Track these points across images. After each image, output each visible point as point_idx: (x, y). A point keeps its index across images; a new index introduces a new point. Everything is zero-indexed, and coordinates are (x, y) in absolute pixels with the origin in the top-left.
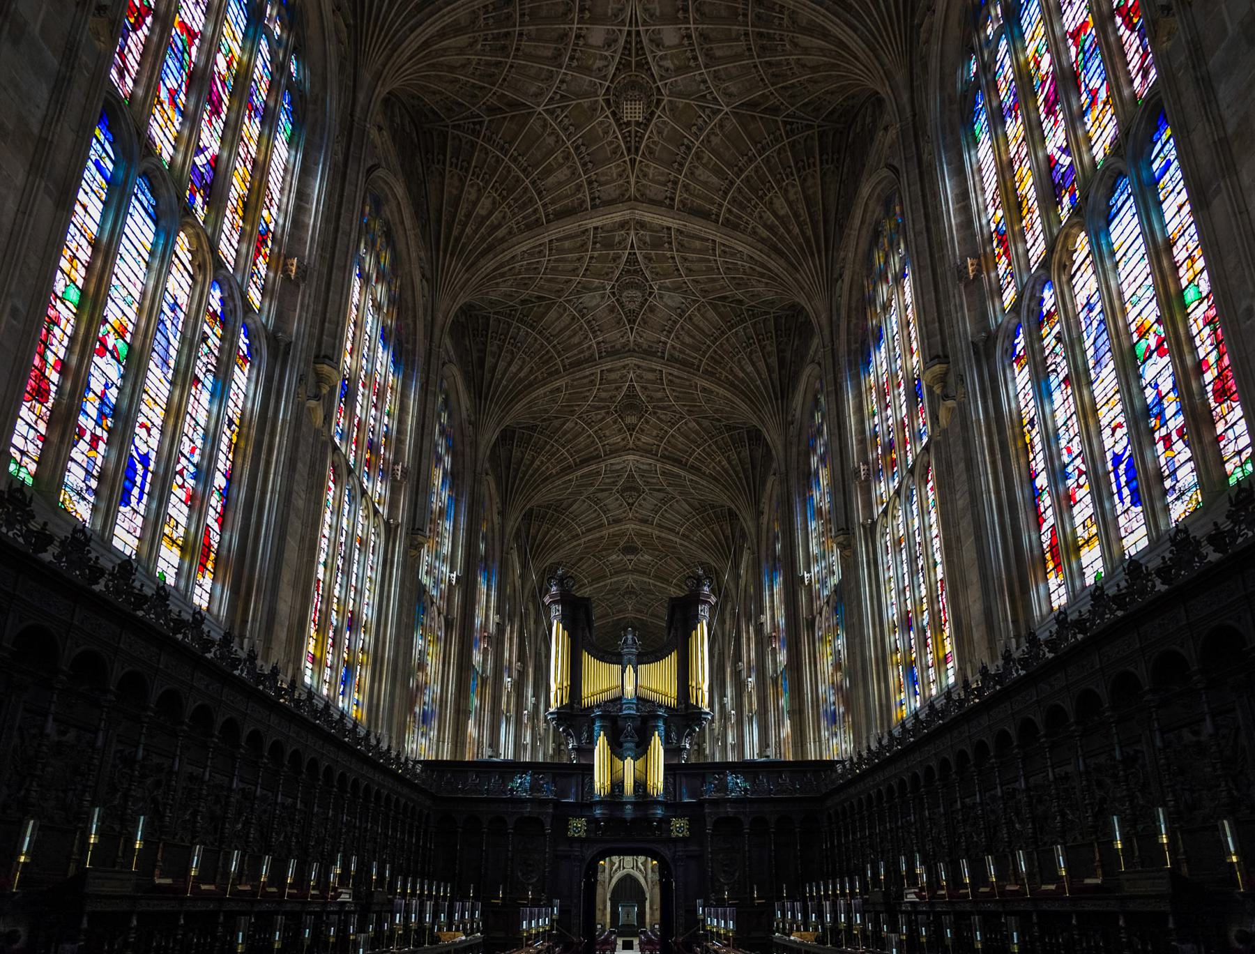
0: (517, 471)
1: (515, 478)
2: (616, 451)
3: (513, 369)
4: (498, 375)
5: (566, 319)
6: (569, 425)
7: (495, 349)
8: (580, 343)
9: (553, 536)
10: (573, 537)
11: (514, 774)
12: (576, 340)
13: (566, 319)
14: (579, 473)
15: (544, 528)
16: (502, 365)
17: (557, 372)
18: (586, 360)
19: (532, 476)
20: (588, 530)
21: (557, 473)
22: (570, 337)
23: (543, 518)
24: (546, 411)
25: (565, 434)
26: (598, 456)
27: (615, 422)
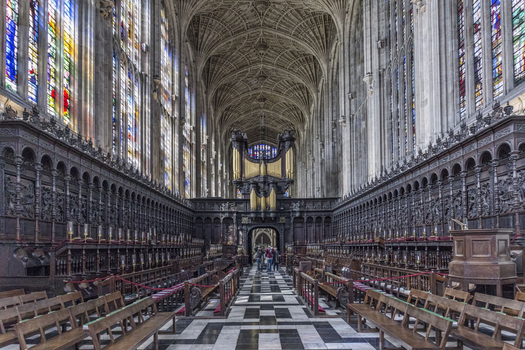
0: (212, 73)
1: (211, 76)
2: (255, 63)
3: (211, 36)
4: (204, 40)
5: (233, 15)
6: (235, 54)
7: (202, 29)
8: (239, 24)
9: (228, 97)
10: (236, 96)
11: (222, 203)
12: (237, 23)
13: (233, 15)
14: (239, 72)
15: (223, 94)
16: (206, 35)
17: (229, 36)
18: (242, 30)
19: (218, 75)
20: (243, 93)
21: (230, 73)
22: (235, 22)
23: (223, 89)
24: (224, 50)
25: (232, 57)
26: (247, 65)
27: (254, 51)
